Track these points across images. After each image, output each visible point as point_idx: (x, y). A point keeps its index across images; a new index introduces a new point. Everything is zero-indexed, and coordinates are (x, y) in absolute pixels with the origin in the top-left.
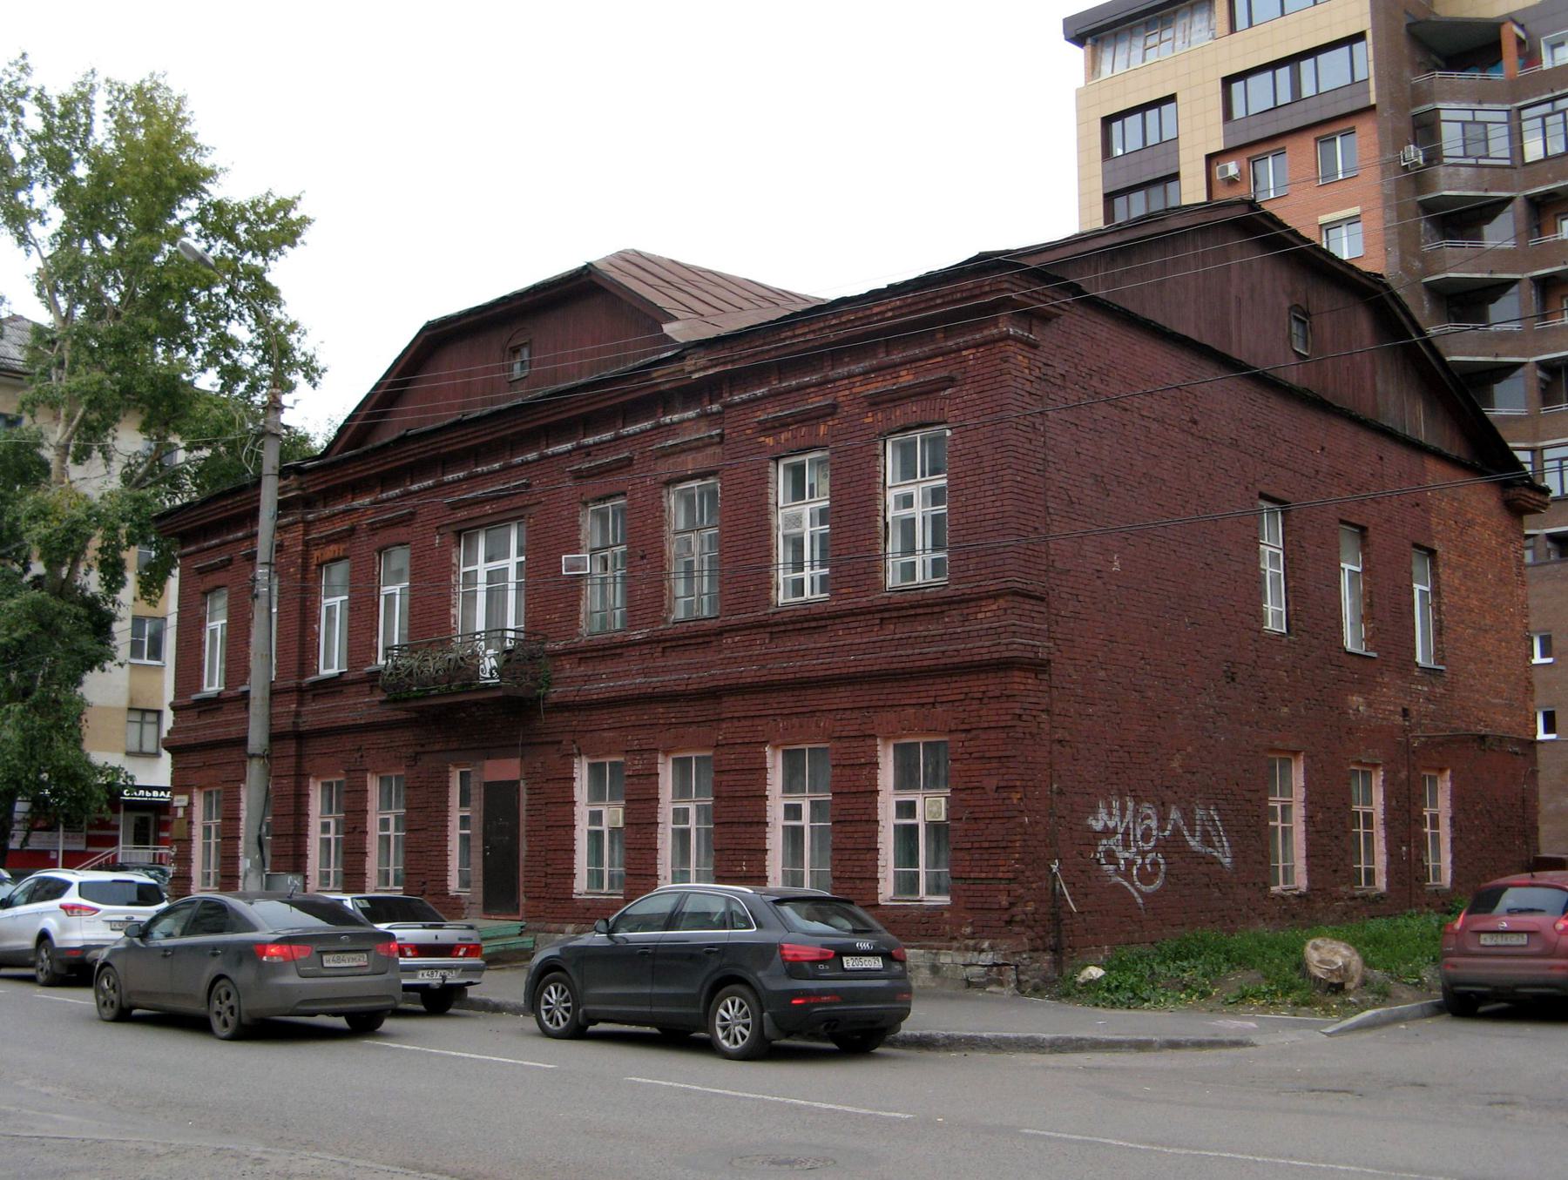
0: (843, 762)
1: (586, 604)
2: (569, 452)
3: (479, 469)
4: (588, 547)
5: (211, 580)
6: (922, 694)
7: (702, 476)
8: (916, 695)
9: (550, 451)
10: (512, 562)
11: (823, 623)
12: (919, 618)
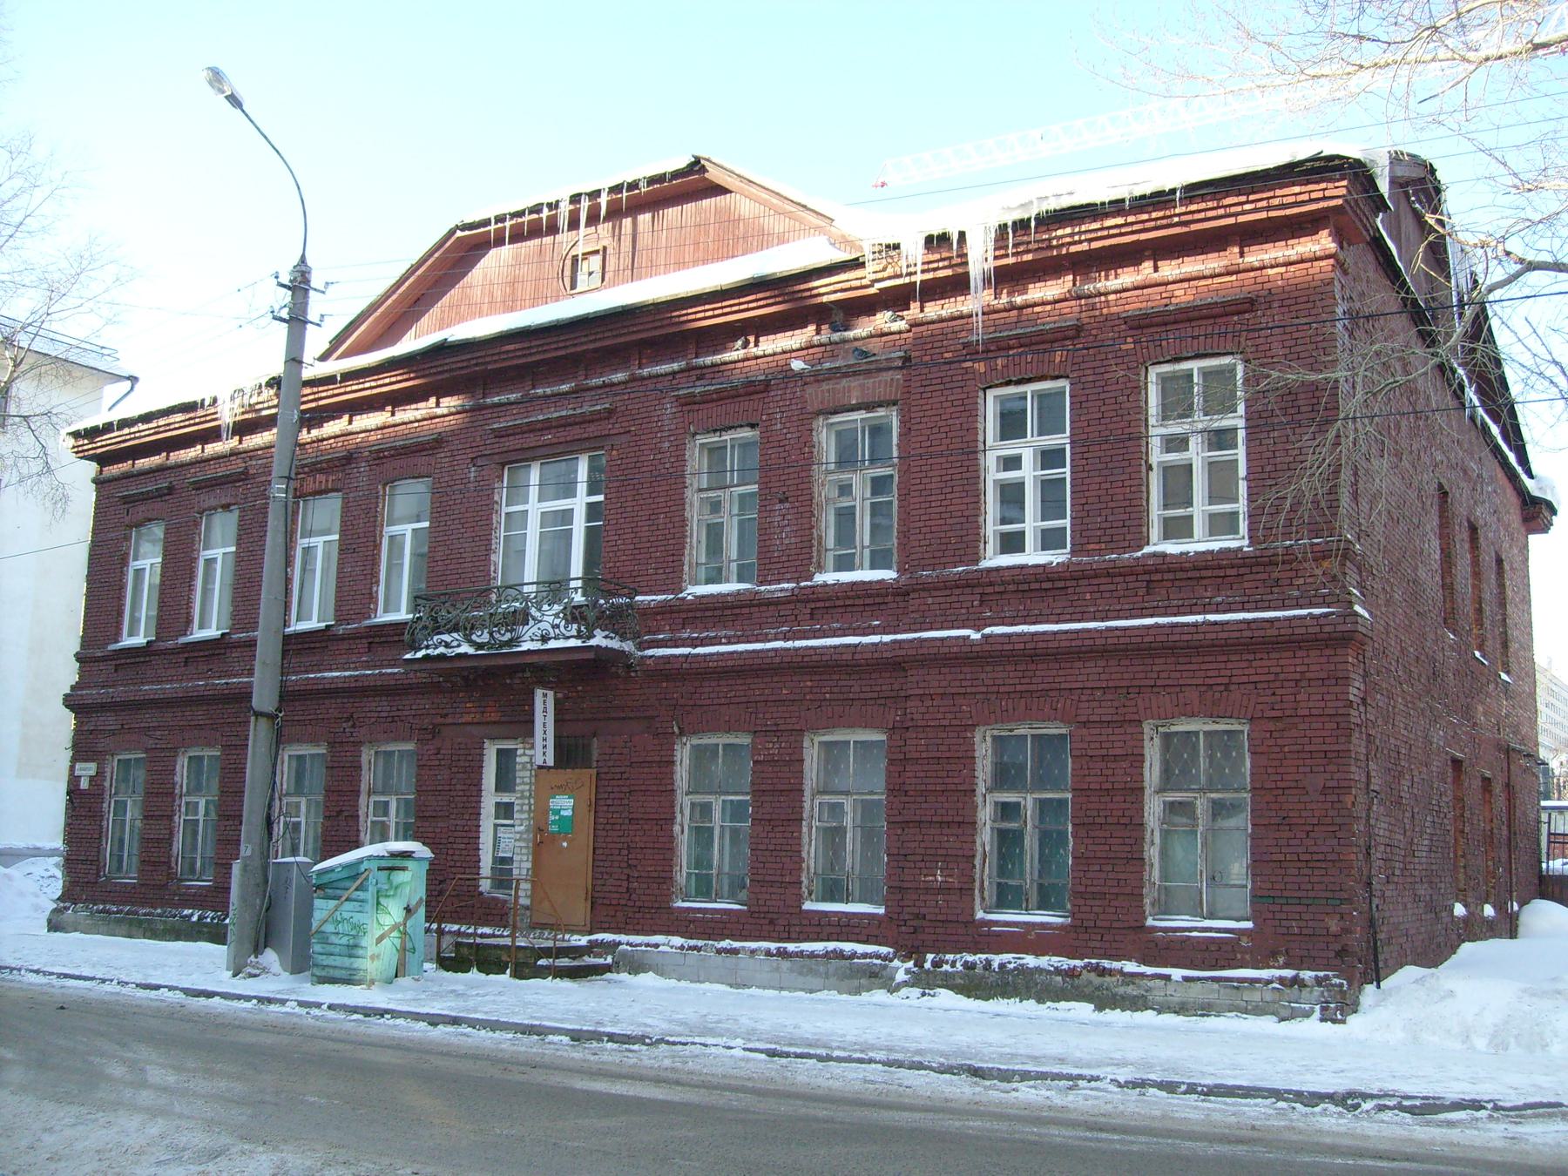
0: (1090, 753)
1: (690, 554)
2: (674, 373)
3: (540, 391)
4: (696, 486)
5: (141, 510)
6: (1210, 673)
7: (869, 407)
8: (1202, 674)
9: (645, 372)
10: (579, 502)
11: (1060, 584)
12: (1204, 582)
